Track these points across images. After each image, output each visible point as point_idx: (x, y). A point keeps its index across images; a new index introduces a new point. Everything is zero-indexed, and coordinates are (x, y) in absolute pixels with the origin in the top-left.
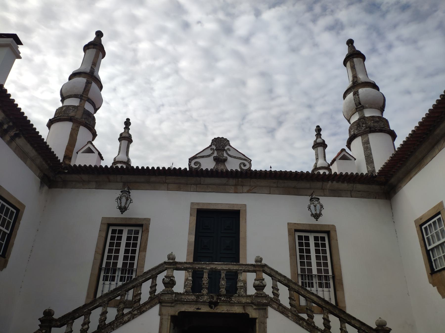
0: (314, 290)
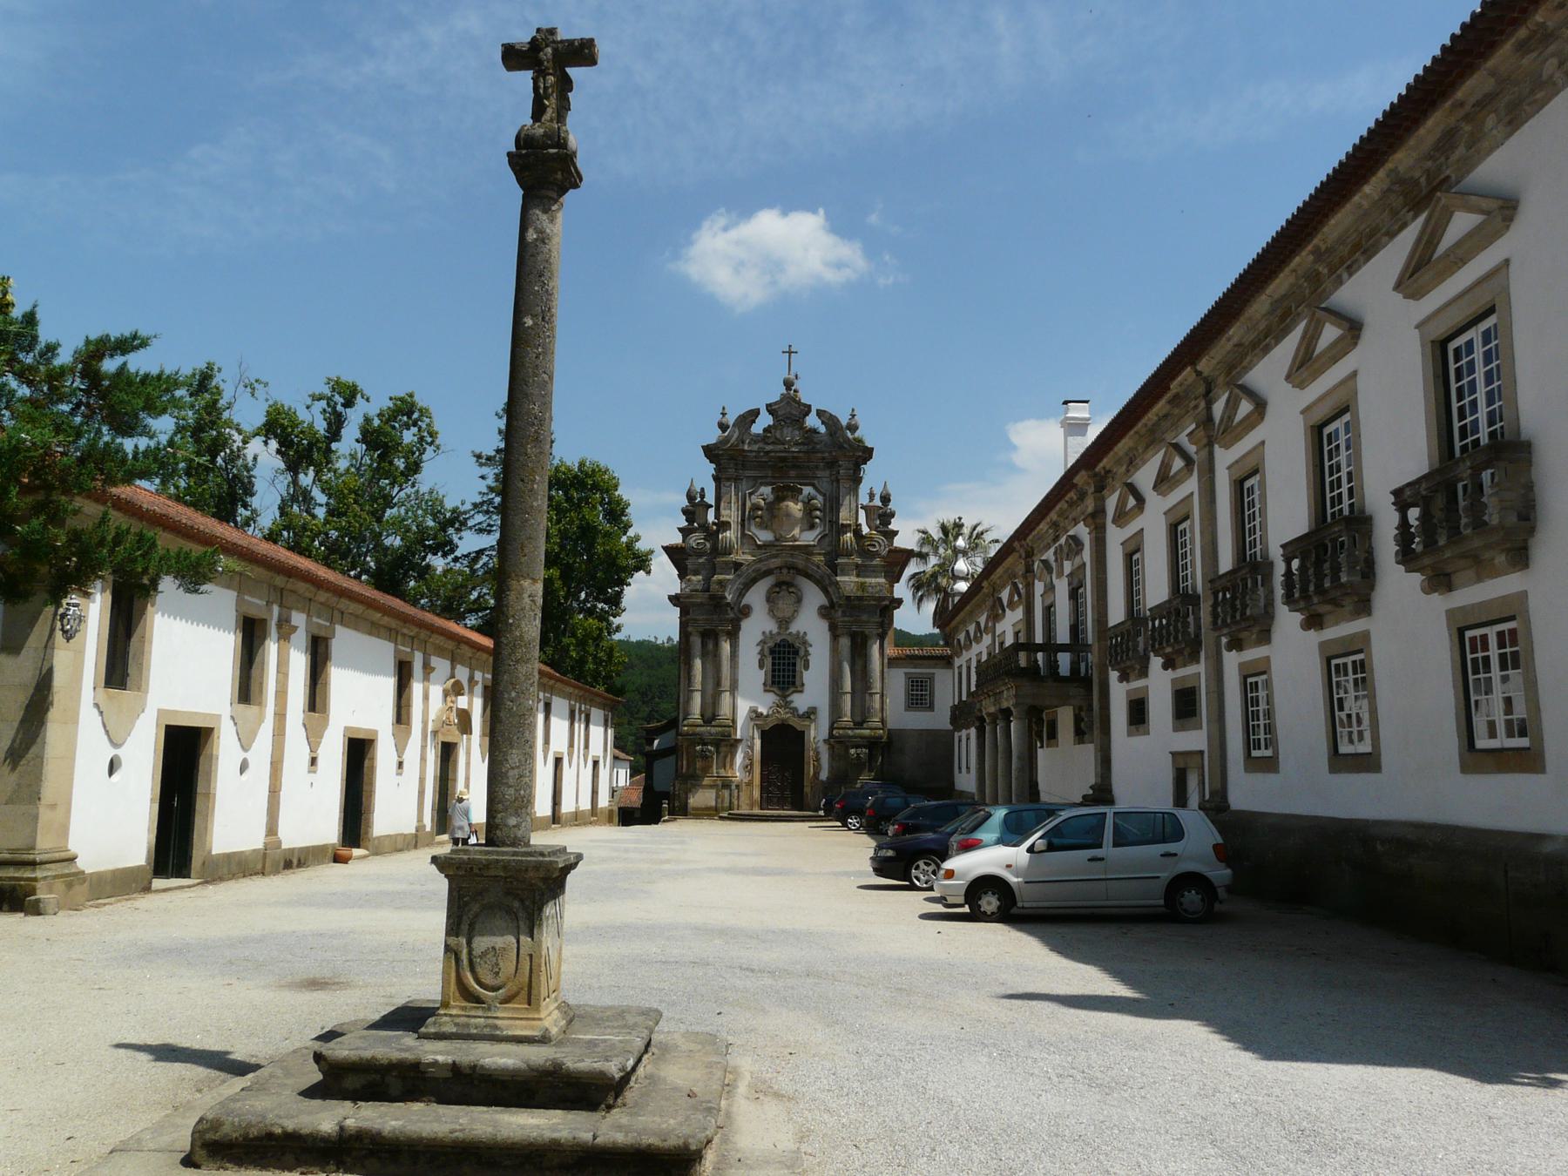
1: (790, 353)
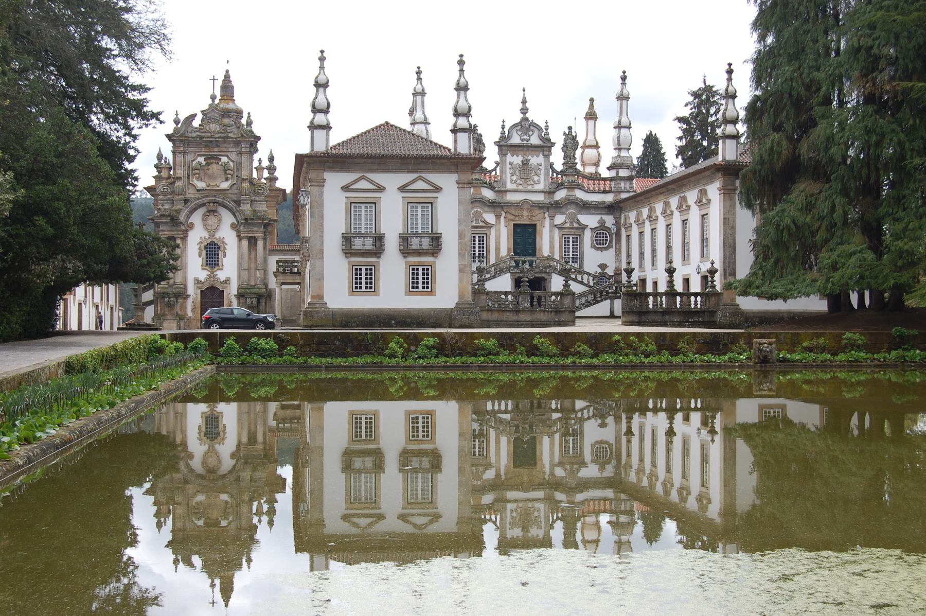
1: (214, 80)
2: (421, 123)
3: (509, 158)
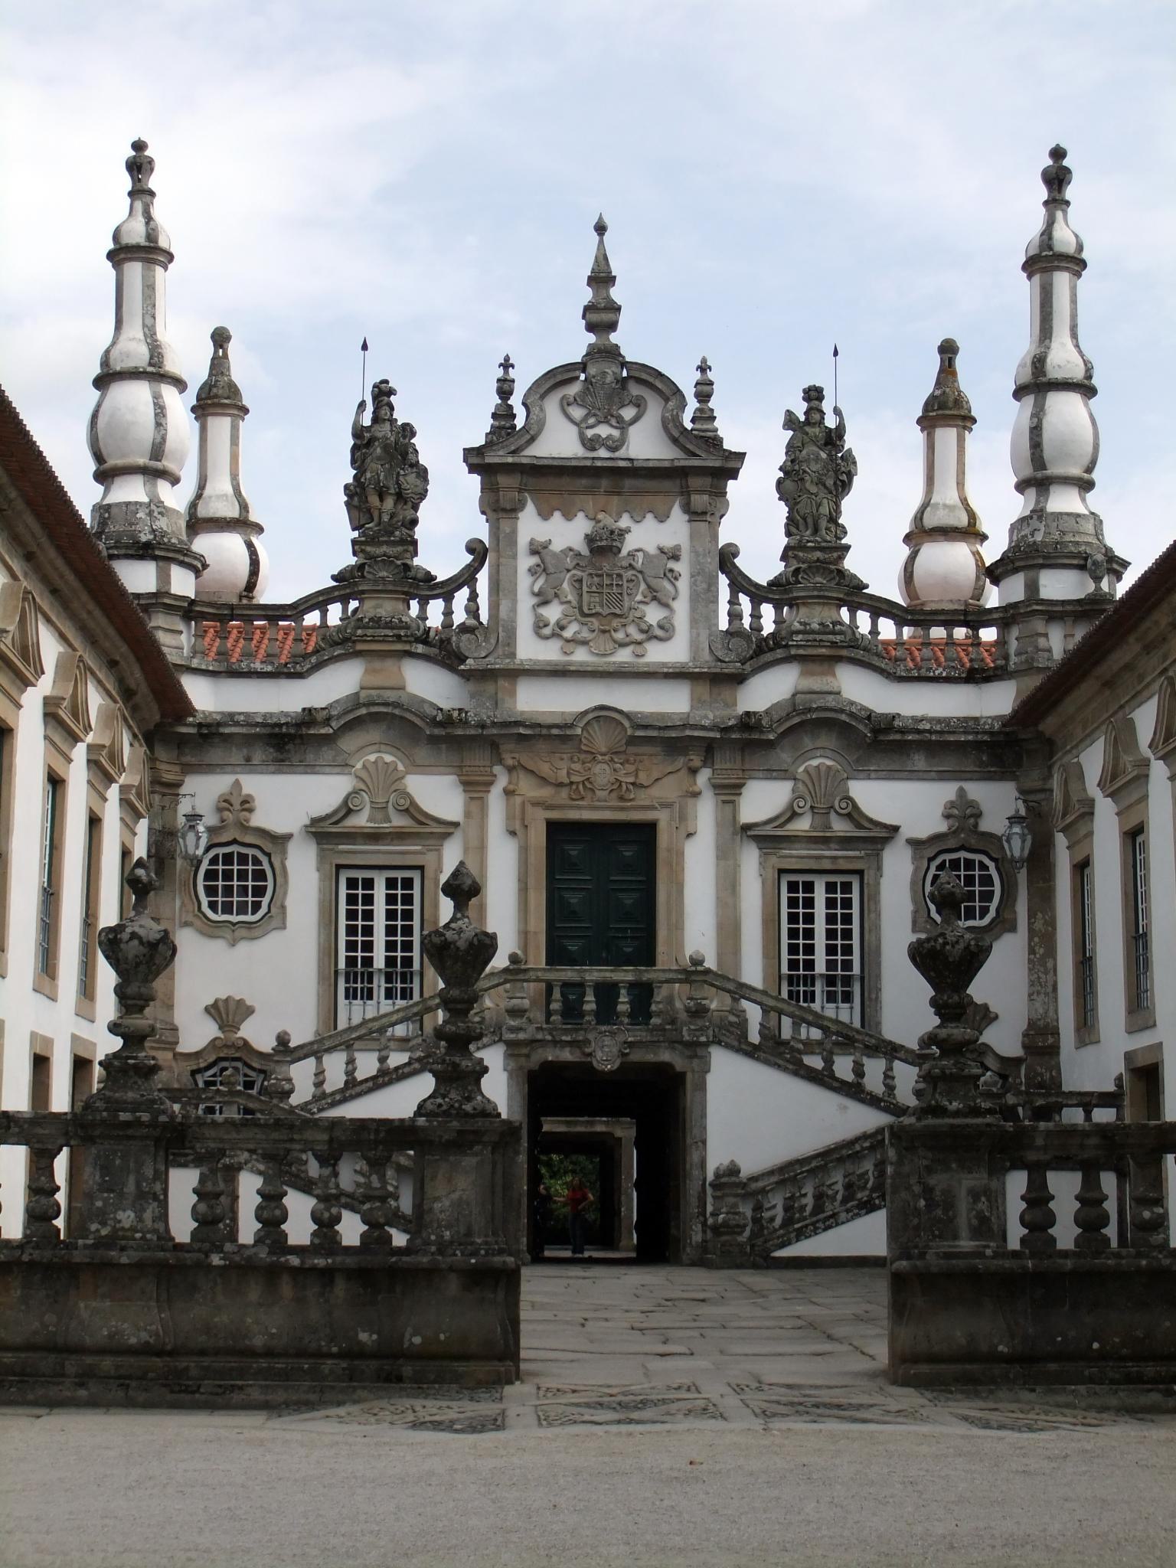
0: (816, 1006)
2: (135, 374)
3: (530, 525)
